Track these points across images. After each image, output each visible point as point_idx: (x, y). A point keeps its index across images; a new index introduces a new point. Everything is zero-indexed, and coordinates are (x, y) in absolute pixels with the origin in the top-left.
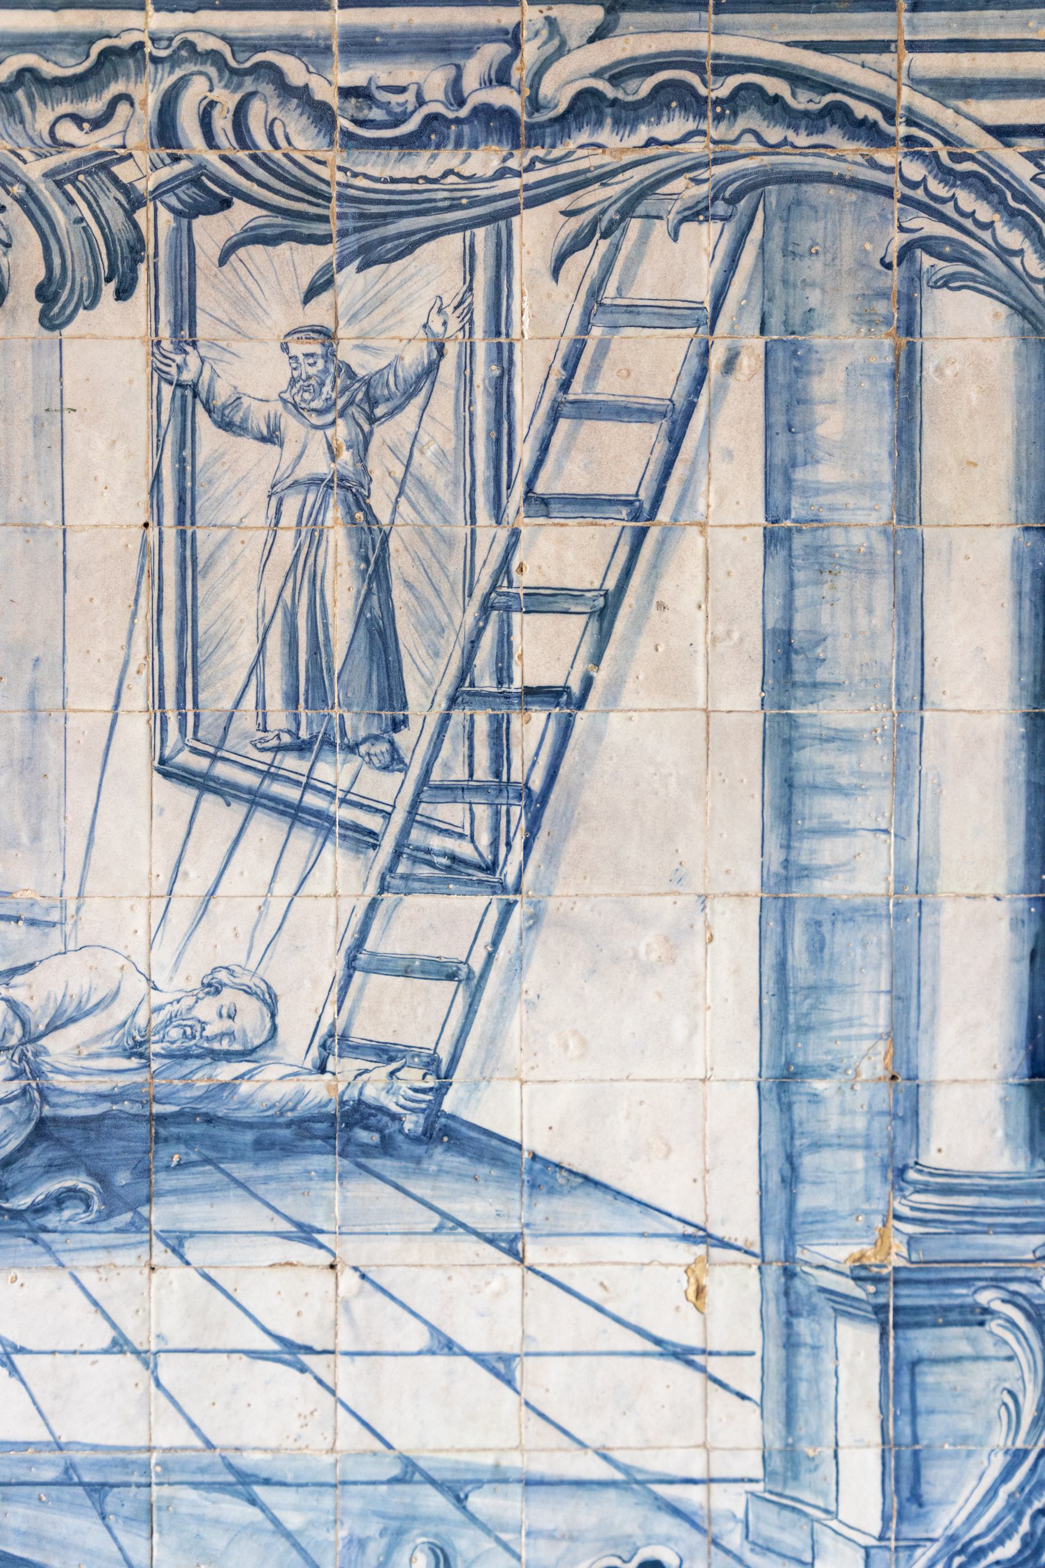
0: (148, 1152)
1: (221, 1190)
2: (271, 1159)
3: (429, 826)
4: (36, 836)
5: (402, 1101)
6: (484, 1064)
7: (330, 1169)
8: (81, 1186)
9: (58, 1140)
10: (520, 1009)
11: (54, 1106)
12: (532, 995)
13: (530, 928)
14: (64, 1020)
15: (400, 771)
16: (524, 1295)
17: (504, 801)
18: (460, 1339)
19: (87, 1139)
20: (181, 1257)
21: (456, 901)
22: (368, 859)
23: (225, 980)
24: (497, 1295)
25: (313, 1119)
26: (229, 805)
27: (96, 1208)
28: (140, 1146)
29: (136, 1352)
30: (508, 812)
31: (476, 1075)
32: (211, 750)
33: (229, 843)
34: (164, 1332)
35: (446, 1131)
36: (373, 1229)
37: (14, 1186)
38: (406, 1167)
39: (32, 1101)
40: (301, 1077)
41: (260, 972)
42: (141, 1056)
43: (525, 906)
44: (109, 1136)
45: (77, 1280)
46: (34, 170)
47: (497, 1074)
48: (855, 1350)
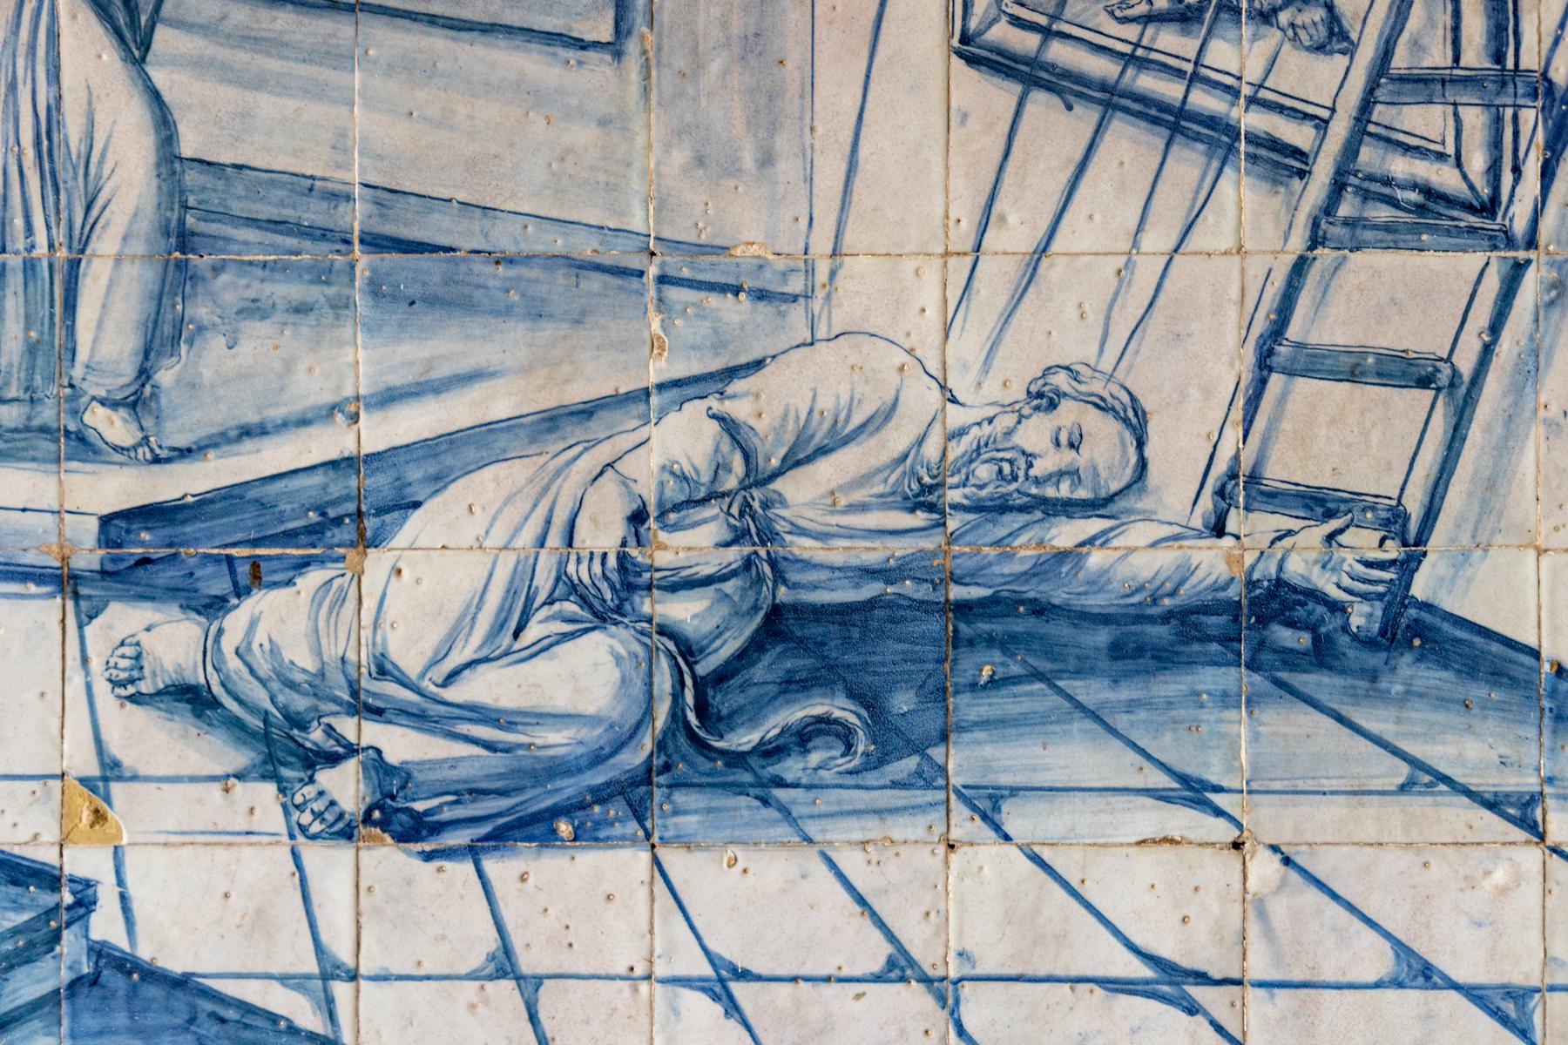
0: (941, 661)
1: (1058, 722)
2: (1138, 672)
3: (1388, 140)
4: (767, 160)
5: (1347, 581)
6: (1478, 522)
7: (1233, 689)
8: (837, 714)
9: (801, 640)
10: (1536, 433)
11: (795, 586)
12: (1555, 411)
13: (1552, 303)
14: (810, 450)
15: (1343, 52)
16: (1546, 892)
17: (1509, 101)
18: (1443, 962)
19: (847, 640)
20: (997, 828)
21: (1433, 262)
22: (1292, 194)
23: (1065, 388)
24: (1503, 891)
25: (1205, 610)
26: (1070, 108)
27: (861, 749)
28: (930, 652)
29: (926, 980)
30: (1515, 117)
31: (1466, 539)
32: (1043, 20)
33: (1070, 170)
34: (968, 948)
35: (1417, 629)
36: (1301, 785)
37: (731, 715)
38: (1354, 687)
39: (760, 579)
40: (1186, 543)
41: (1120, 375)
42: (931, 508)
43: (1544, 269)
44: (882, 634)
45: (832, 864)
47: (1498, 539)
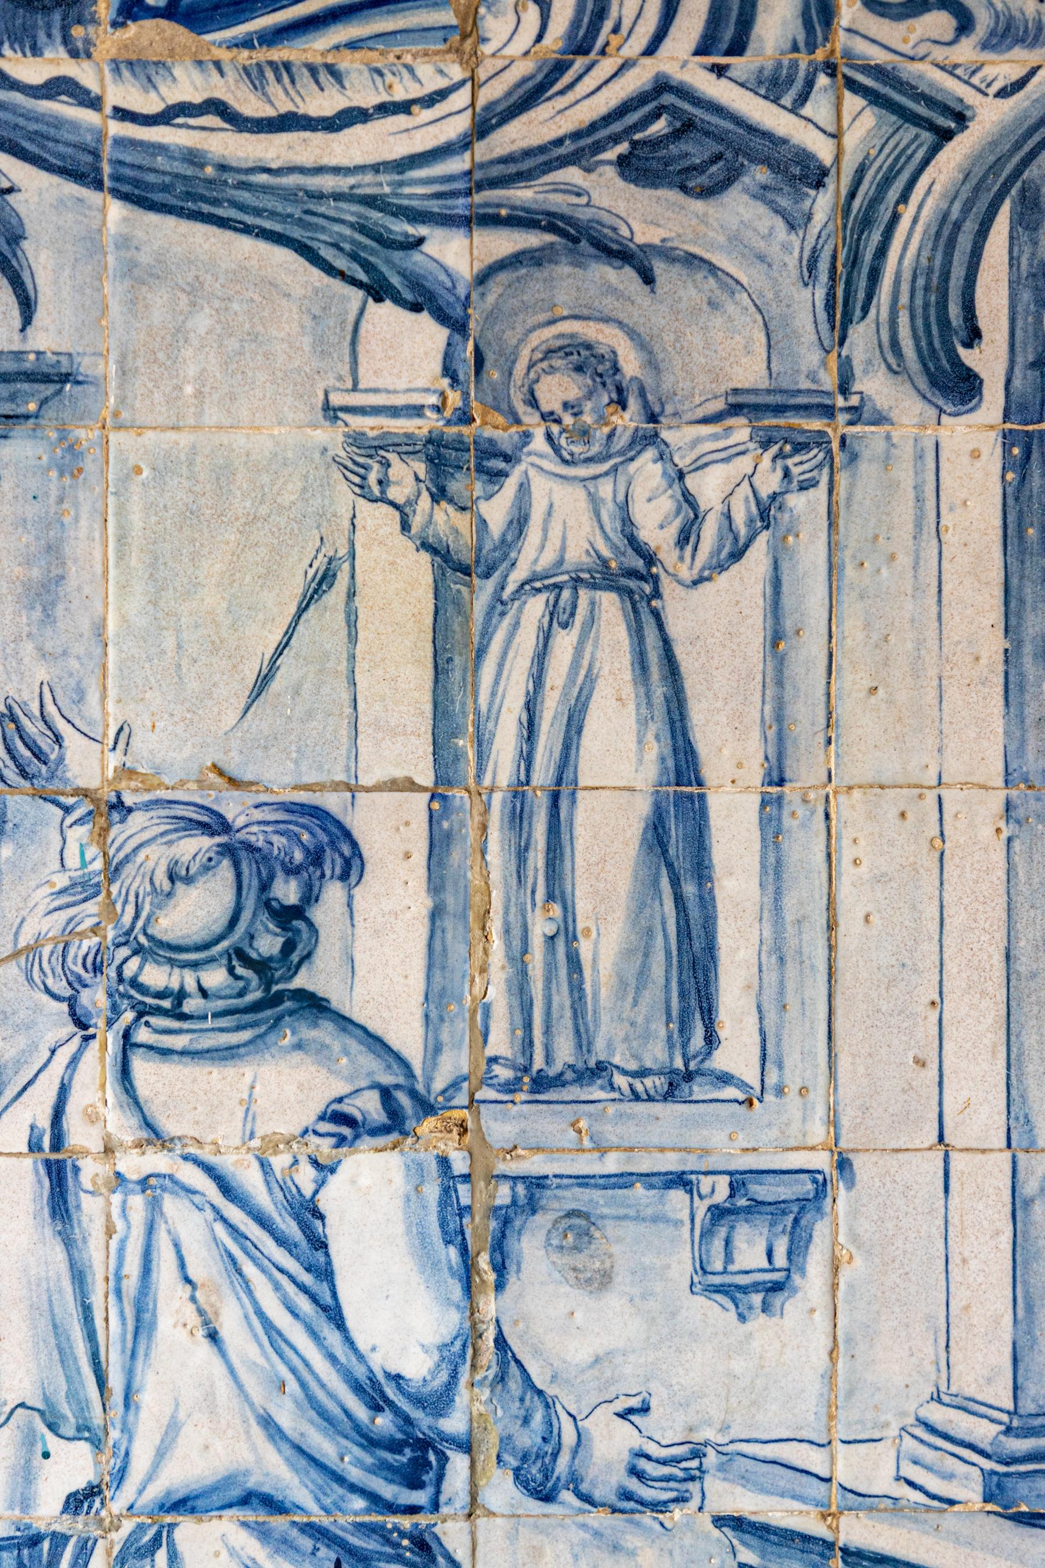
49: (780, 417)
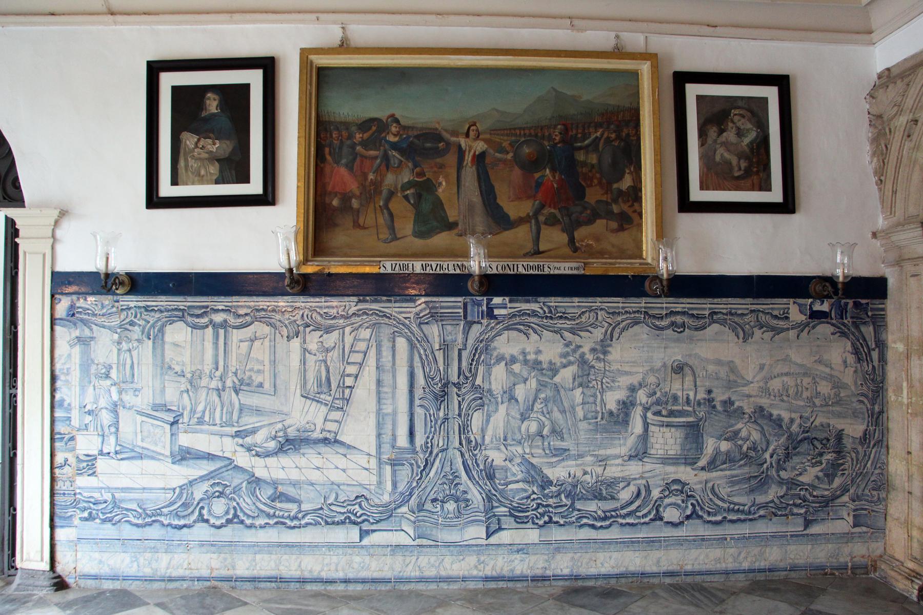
46: (286, 322)
48: (388, 469)
49: (138, 340)
